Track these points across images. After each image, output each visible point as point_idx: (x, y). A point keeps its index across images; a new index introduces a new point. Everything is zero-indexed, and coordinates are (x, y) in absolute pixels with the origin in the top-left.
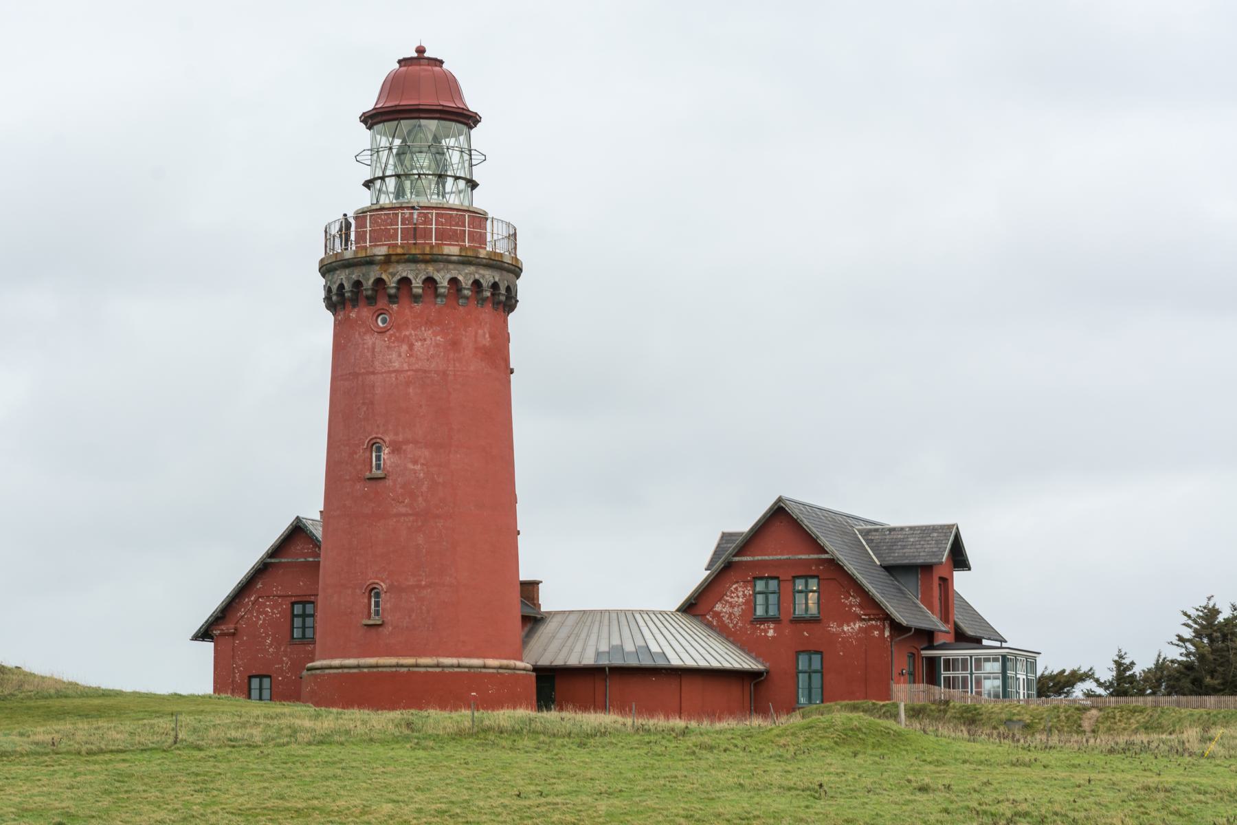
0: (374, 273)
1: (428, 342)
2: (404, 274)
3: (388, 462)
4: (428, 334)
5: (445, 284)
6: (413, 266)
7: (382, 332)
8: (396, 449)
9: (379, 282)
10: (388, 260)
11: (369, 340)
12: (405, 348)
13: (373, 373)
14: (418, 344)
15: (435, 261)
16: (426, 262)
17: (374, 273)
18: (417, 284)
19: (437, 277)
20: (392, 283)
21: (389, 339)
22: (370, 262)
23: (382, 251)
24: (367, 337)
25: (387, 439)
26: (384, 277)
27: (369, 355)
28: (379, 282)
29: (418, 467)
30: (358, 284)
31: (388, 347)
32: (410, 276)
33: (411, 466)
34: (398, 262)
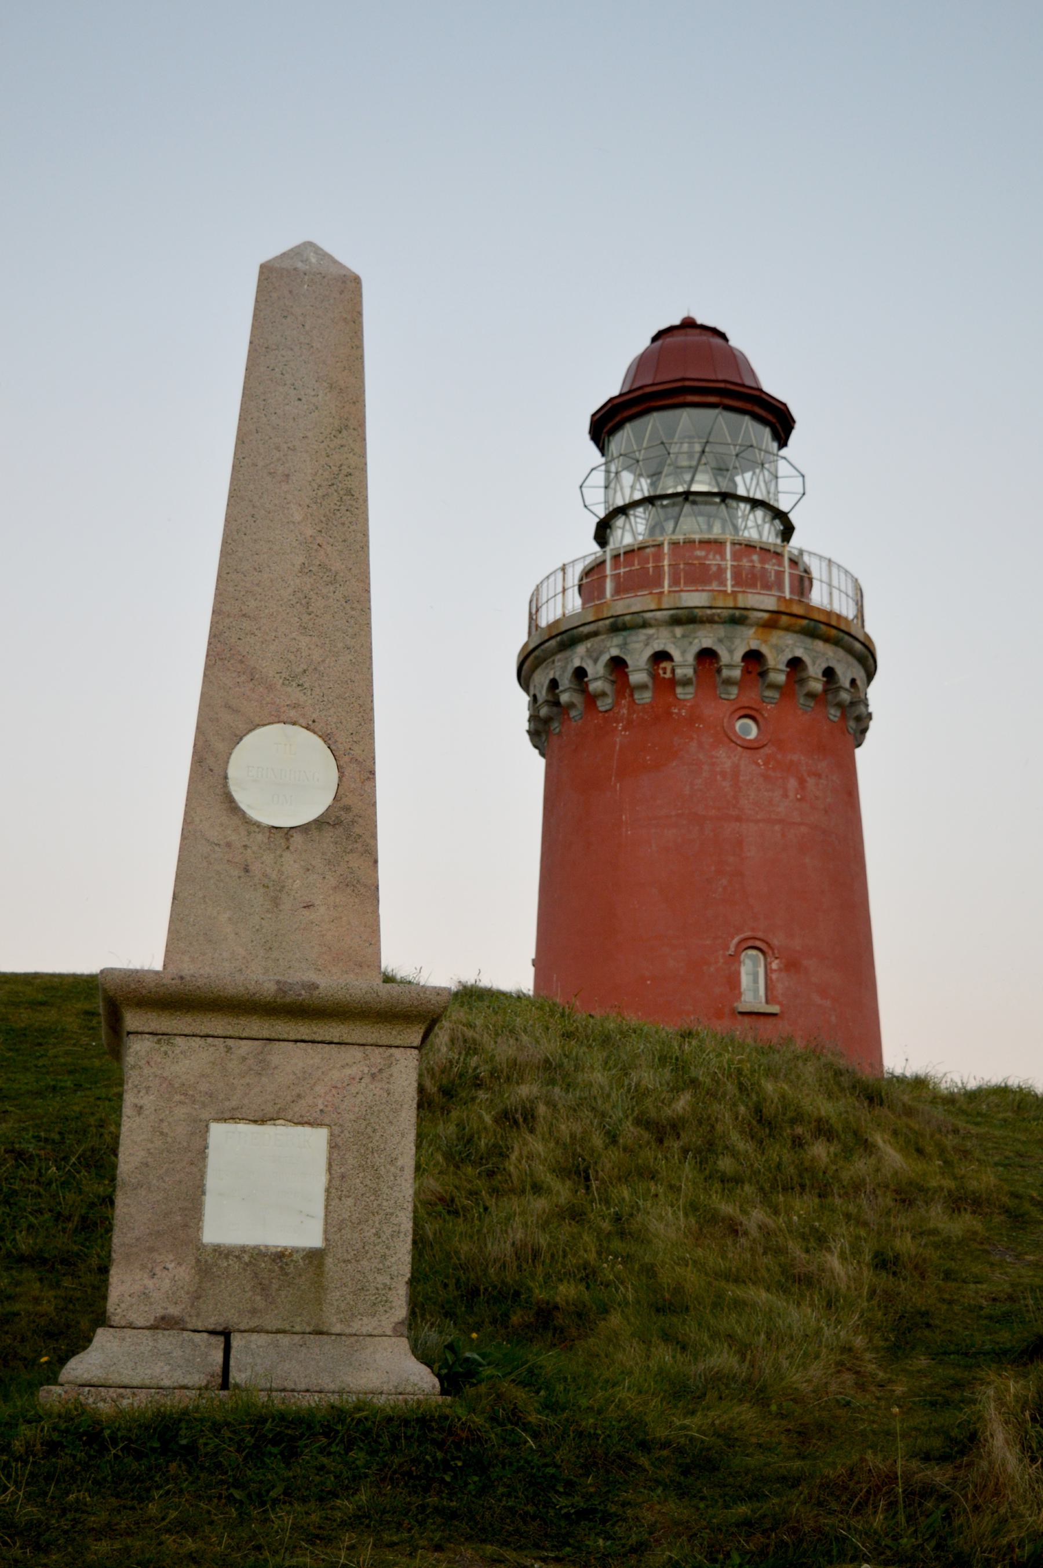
0: (748, 639)
1: (823, 781)
2: (799, 653)
3: (780, 988)
4: (823, 765)
5: (847, 685)
6: (808, 641)
7: (752, 747)
8: (792, 965)
9: (753, 657)
10: (772, 622)
11: (725, 758)
12: (792, 783)
13: (738, 819)
14: (811, 782)
15: (837, 643)
16: (827, 640)
17: (748, 639)
18: (814, 670)
19: (839, 670)
20: (776, 661)
21: (766, 763)
22: (737, 619)
23: (769, 602)
24: (721, 753)
25: (775, 942)
26: (765, 650)
27: (726, 784)
28: (753, 657)
29: (828, 1003)
30: (707, 656)
31: (766, 778)
32: (806, 659)
33: (817, 999)
34: (787, 629)
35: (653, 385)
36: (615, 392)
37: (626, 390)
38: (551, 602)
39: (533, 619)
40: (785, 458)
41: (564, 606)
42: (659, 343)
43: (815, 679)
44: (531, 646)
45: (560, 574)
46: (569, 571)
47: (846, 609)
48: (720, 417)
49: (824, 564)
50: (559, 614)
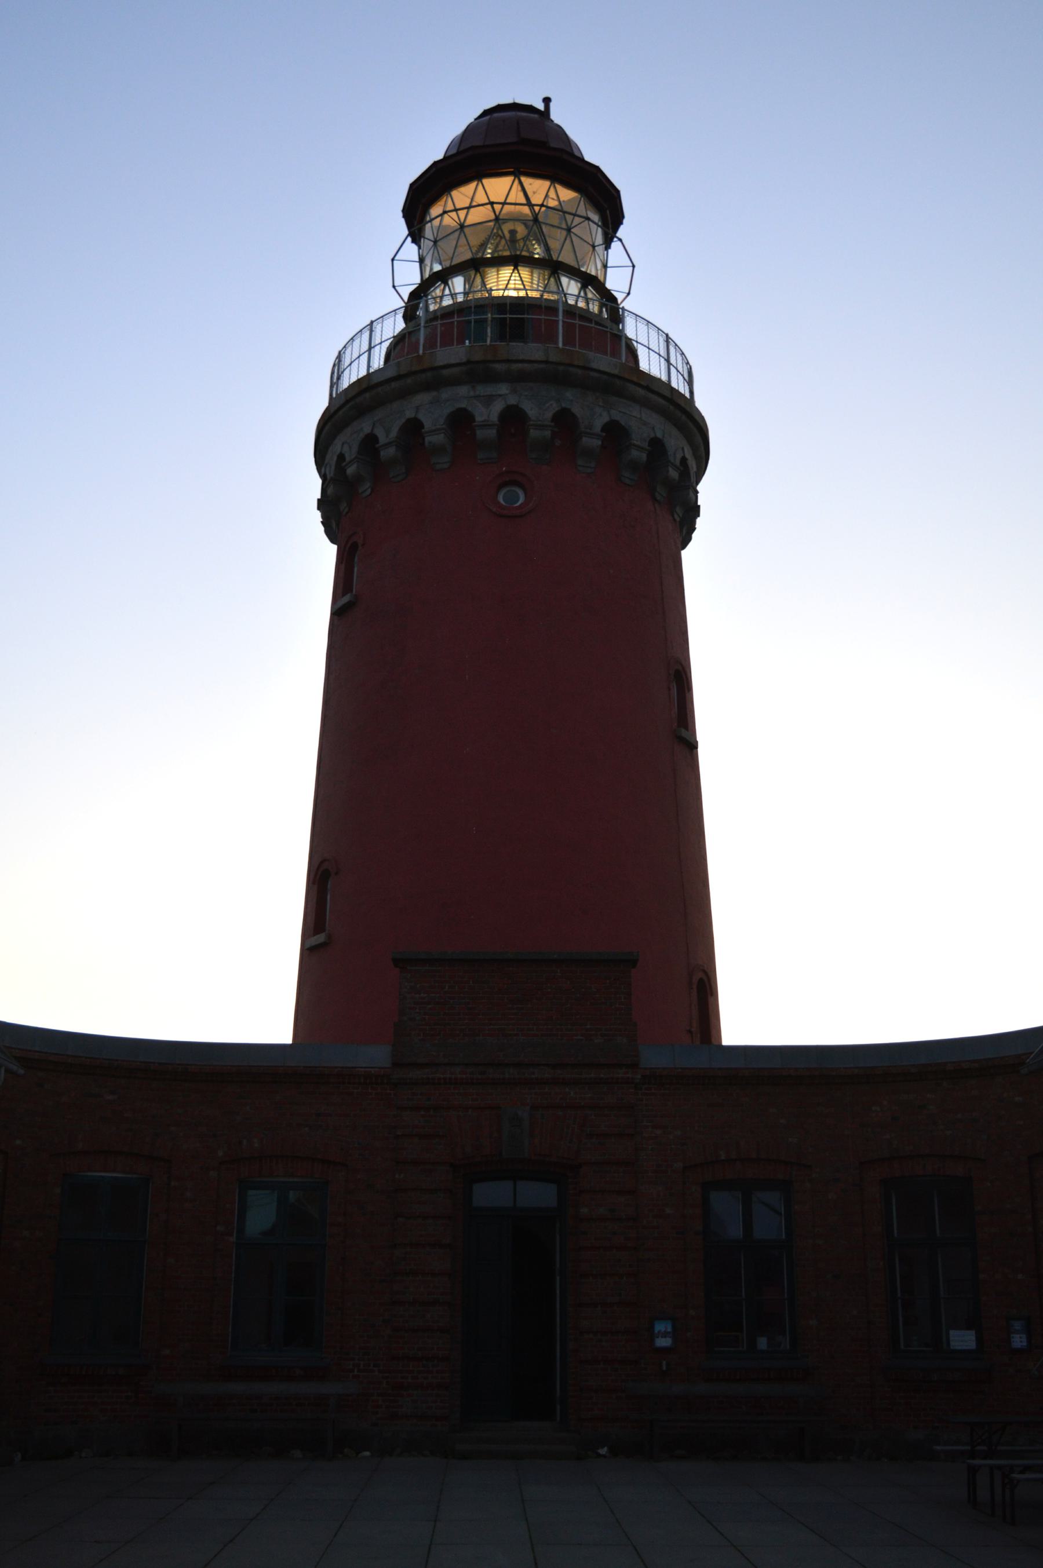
35: (483, 146)
36: (439, 155)
37: (449, 154)
38: (355, 364)
39: (334, 383)
40: (620, 240)
41: (369, 366)
42: (487, 118)
43: (647, 454)
44: (332, 411)
45: (366, 335)
46: (378, 328)
47: (683, 388)
48: (552, 189)
49: (662, 340)
50: (363, 373)
